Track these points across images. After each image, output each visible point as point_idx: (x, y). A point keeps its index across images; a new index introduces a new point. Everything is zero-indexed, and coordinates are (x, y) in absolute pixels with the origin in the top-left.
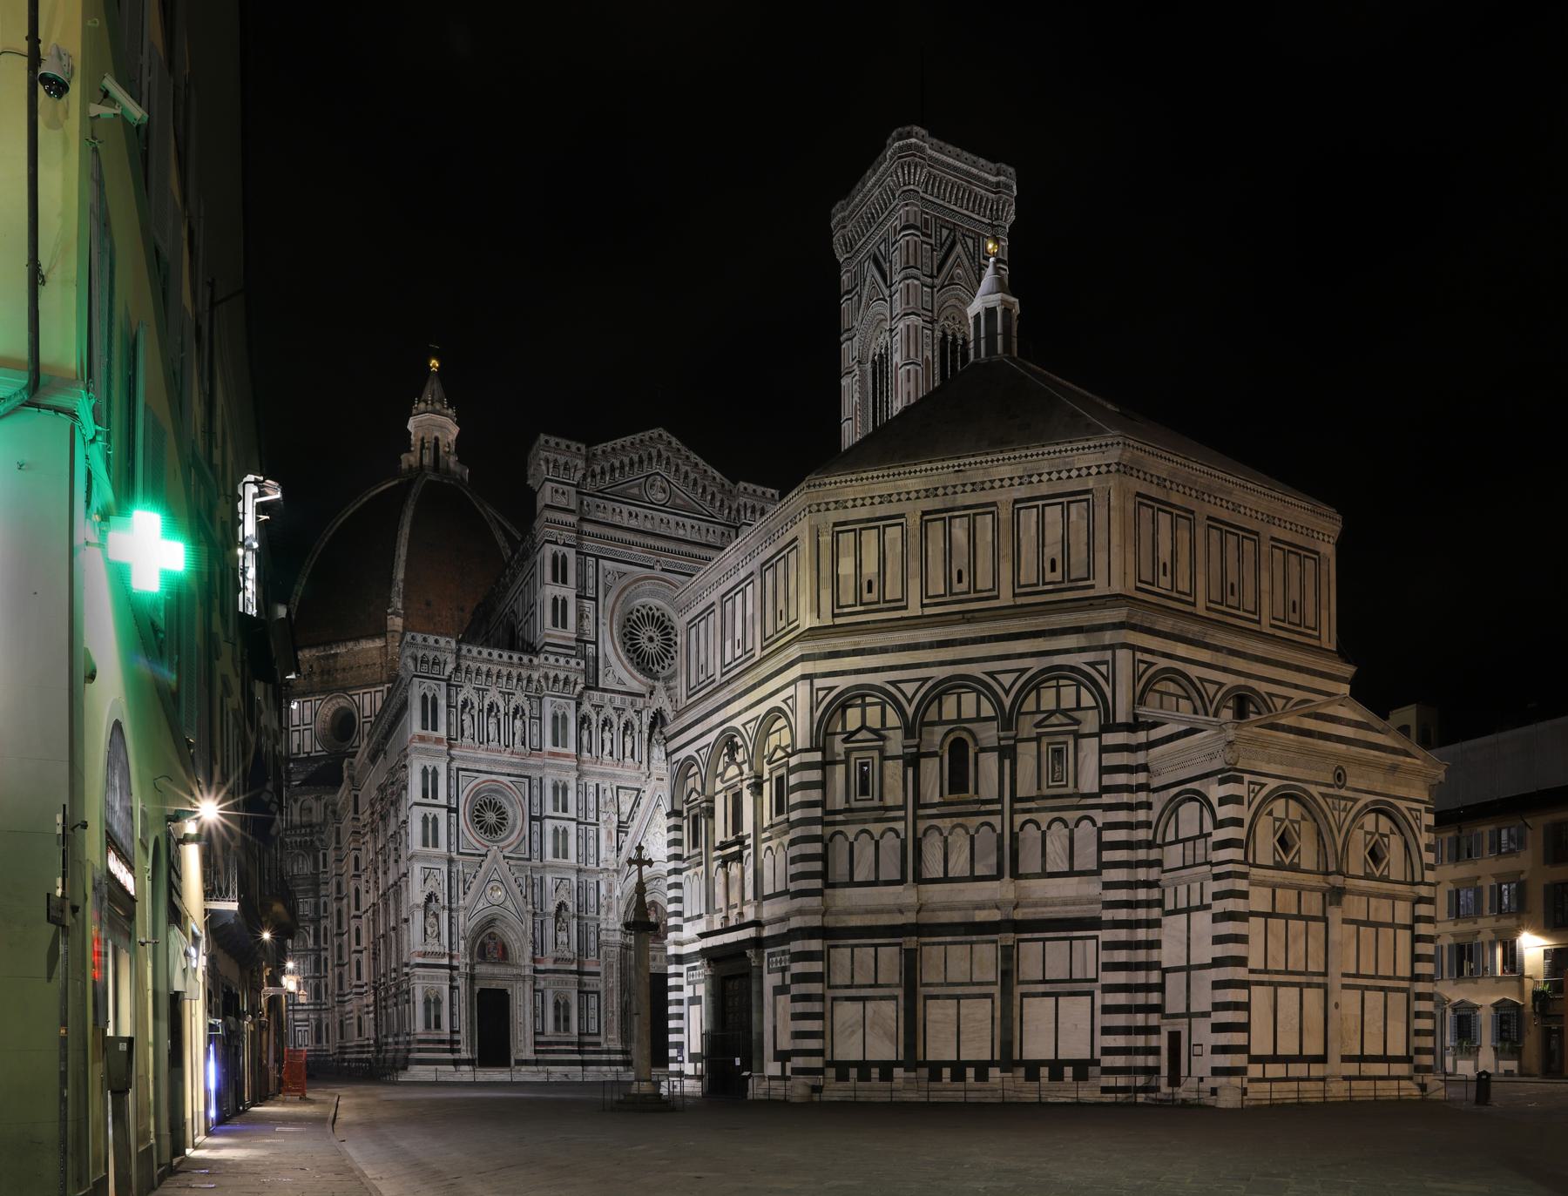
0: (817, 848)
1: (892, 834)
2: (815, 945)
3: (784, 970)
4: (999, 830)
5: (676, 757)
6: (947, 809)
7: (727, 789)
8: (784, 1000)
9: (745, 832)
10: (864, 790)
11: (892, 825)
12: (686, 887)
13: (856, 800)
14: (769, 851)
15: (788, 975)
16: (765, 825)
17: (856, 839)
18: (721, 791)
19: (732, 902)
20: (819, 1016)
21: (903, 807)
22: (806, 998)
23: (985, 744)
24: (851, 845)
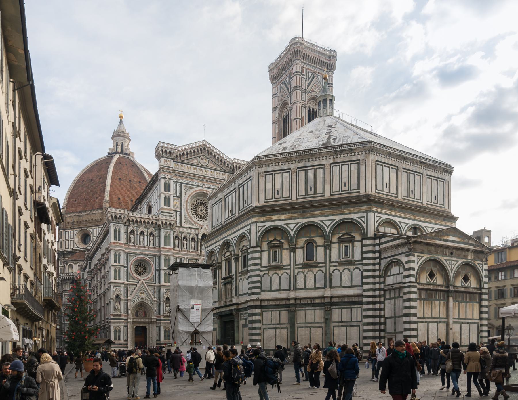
0: (259, 279)
1: (286, 274)
2: (258, 311)
4: (325, 272)
5: (207, 249)
6: (305, 266)
7: (226, 260)
10: (275, 260)
11: (286, 271)
14: (241, 280)
16: (240, 271)
17: (272, 276)
19: (228, 297)
21: (290, 265)
23: (318, 244)
24: (271, 277)
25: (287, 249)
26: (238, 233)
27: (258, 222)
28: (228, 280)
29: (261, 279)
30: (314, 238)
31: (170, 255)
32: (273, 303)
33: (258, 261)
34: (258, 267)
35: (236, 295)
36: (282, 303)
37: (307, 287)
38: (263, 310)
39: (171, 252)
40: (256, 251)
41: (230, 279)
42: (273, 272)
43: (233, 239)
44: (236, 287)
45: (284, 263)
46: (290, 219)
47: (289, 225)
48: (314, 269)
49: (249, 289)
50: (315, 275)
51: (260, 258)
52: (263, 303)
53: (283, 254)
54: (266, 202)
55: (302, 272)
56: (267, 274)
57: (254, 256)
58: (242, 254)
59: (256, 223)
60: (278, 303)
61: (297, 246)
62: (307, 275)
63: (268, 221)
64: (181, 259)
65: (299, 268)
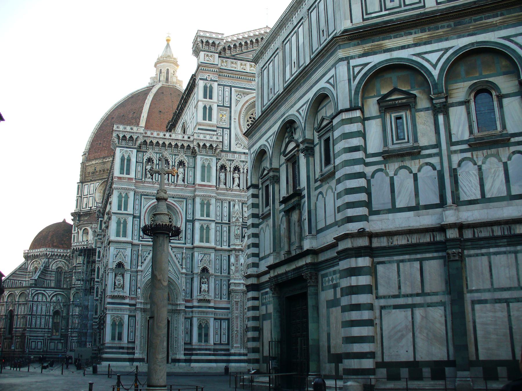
0: (361, 182)
1: (430, 168)
2: (363, 262)
3: (335, 286)
5: (252, 150)
7: (288, 160)
8: (336, 311)
9: (302, 186)
11: (428, 160)
12: (261, 236)
13: (393, 144)
15: (338, 290)
16: (317, 177)
18: (284, 163)
20: (369, 323)
21: (438, 145)
22: (357, 307)
23: (504, 92)
24: (392, 179)
25: (427, 109)
26: (310, 95)
27: (352, 58)
28: (293, 201)
29: (369, 182)
30: (490, 79)
31: (210, 196)
32: (401, 241)
33: (356, 142)
34: (359, 155)
35: (310, 232)
36: (427, 239)
37: (488, 196)
38: (376, 260)
39: (212, 191)
40: (351, 119)
41: (296, 199)
42: (396, 165)
43: (300, 111)
44: (309, 212)
45: (423, 141)
46: (425, 44)
47: (426, 56)
48: (501, 150)
49: (339, 210)
50: (505, 165)
51: (363, 134)
52: (376, 243)
53: (418, 120)
54: (368, 19)
55: (471, 159)
56: (381, 170)
57: (347, 131)
58: (320, 138)
59: (347, 59)
60: (414, 239)
61: (450, 101)
62: (484, 167)
63: (375, 53)
64: (229, 202)
65: (462, 151)
